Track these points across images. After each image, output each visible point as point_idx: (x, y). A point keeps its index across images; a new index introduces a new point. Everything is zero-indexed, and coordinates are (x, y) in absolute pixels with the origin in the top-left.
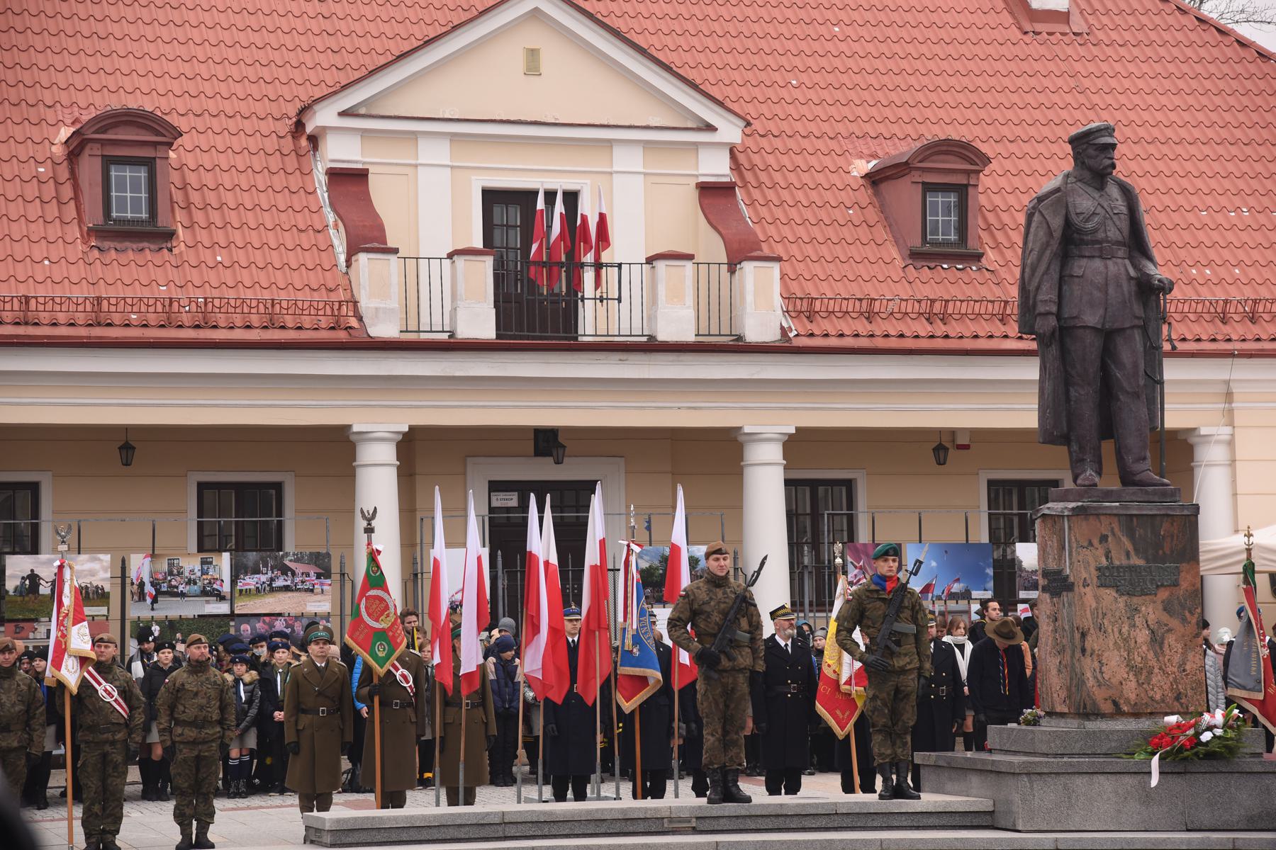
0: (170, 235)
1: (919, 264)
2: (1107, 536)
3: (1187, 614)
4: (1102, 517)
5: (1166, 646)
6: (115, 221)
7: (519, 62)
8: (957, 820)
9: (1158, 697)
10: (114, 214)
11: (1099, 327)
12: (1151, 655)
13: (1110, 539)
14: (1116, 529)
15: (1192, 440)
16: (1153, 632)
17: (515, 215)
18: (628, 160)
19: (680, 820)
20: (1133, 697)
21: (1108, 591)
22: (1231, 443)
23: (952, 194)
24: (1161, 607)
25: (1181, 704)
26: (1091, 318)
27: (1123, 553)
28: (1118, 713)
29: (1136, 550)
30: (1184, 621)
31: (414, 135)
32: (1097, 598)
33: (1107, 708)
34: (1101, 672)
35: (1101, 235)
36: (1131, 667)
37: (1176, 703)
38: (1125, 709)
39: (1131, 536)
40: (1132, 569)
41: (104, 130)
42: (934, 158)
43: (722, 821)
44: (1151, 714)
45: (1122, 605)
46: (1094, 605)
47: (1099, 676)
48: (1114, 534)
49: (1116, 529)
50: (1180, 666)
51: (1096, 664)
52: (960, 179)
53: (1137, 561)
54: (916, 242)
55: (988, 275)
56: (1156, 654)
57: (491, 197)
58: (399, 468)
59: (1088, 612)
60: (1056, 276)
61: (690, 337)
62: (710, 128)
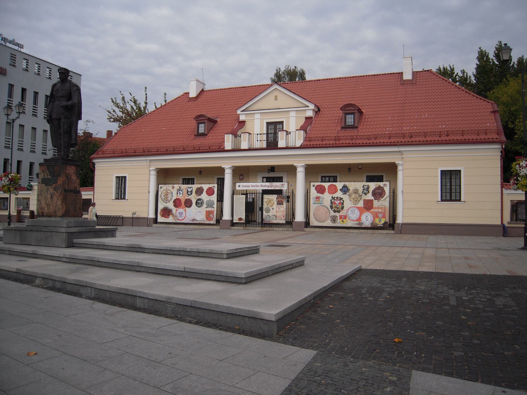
1: (344, 129)
2: (44, 171)
4: (44, 166)
6: (199, 133)
9: (51, 212)
12: (50, 201)
13: (45, 172)
14: (46, 169)
16: (51, 195)
18: (293, 114)
20: (46, 211)
21: (44, 185)
23: (353, 115)
24: (53, 188)
25: (55, 214)
32: (41, 186)
34: (41, 205)
36: (46, 204)
37: (54, 214)
38: (45, 215)
40: (48, 179)
42: (347, 108)
45: (45, 188)
46: (40, 188)
47: (40, 206)
49: (46, 169)
50: (56, 204)
51: (40, 203)
53: (50, 177)
54: (343, 125)
56: (51, 201)
57: (268, 124)
61: (285, 146)
62: (308, 107)
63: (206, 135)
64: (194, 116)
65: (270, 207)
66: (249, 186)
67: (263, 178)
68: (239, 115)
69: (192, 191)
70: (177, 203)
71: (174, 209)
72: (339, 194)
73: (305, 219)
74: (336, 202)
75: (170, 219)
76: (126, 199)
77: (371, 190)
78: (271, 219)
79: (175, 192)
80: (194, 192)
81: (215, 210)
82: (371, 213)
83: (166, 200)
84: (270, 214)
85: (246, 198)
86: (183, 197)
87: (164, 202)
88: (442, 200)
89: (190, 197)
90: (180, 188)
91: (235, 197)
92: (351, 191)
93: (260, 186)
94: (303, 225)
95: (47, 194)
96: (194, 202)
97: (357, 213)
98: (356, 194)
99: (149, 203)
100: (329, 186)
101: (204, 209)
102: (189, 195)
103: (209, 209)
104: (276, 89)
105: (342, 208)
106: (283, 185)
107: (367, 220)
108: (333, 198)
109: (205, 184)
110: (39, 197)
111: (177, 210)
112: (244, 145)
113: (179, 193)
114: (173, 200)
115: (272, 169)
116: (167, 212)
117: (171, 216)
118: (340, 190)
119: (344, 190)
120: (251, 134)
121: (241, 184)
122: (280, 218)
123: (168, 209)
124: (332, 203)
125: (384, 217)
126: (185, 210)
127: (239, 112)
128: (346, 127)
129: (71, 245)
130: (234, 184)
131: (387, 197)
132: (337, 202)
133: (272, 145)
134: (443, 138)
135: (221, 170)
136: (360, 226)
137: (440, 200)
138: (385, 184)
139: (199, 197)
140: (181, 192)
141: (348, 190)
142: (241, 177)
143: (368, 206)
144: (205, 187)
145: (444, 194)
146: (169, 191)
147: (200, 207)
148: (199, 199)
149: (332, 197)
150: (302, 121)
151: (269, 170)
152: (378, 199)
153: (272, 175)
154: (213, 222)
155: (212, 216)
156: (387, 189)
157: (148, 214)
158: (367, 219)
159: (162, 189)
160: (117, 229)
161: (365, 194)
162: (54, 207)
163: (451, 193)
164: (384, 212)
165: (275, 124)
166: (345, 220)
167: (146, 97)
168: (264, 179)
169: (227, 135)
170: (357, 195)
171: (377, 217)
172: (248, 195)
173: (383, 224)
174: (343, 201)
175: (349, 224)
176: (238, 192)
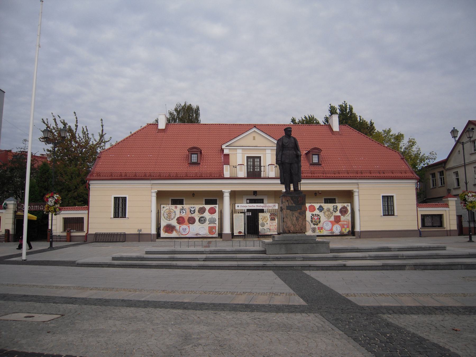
0: (199, 164)
3: (303, 214)
5: (299, 221)
7: (252, 138)
8: (258, 252)
9: (297, 230)
10: (192, 161)
11: (289, 163)
13: (289, 201)
15: (353, 192)
16: (297, 218)
17: (251, 160)
19: (207, 252)
20: (293, 230)
21: (288, 210)
22: (358, 192)
24: (298, 213)
26: (287, 161)
27: (292, 204)
28: (289, 232)
29: (294, 203)
30: (303, 216)
32: (286, 212)
33: (287, 231)
34: (287, 225)
35: (289, 146)
38: (291, 232)
39: (293, 201)
43: (214, 252)
44: (296, 233)
45: (291, 213)
47: (286, 226)
48: (290, 200)
52: (318, 153)
53: (294, 205)
54: (311, 163)
55: (322, 167)
56: (297, 222)
58: (230, 197)
59: (284, 214)
60: (281, 154)
65: (265, 222)
66: (247, 207)
69: (195, 210)
70: (180, 221)
71: (178, 226)
72: (317, 212)
73: (231, 232)
74: (315, 218)
75: (174, 234)
76: (126, 217)
77: (339, 208)
78: (266, 231)
79: (178, 211)
80: (197, 211)
81: (217, 225)
82: (340, 225)
83: (169, 218)
84: (265, 228)
87: (167, 220)
88: (384, 215)
89: (193, 215)
90: (183, 208)
91: (234, 215)
92: (325, 209)
93: (256, 206)
94: (156, 236)
95: (293, 217)
96: (197, 219)
97: (330, 225)
98: (329, 212)
99: (151, 221)
100: (310, 206)
101: (206, 225)
102: (193, 214)
105: (320, 222)
106: (274, 205)
107: (337, 230)
108: (313, 215)
109: (197, 204)
110: (284, 219)
111: (180, 227)
113: (182, 212)
114: (176, 218)
115: (255, 193)
116: (170, 228)
117: (174, 232)
118: (317, 209)
119: (320, 209)
121: (239, 205)
122: (273, 231)
123: (172, 226)
124: (312, 218)
125: (348, 227)
126: (189, 227)
127: (224, 147)
130: (232, 205)
131: (349, 214)
132: (316, 218)
134: (382, 175)
135: (220, 194)
136: (332, 234)
138: (348, 205)
139: (202, 215)
140: (184, 211)
141: (323, 209)
143: (337, 220)
146: (172, 211)
147: (203, 223)
148: (202, 217)
149: (312, 214)
152: (343, 215)
154: (216, 235)
155: (215, 231)
157: (151, 231)
158: (337, 229)
159: (165, 209)
161: (335, 212)
162: (300, 226)
163: (388, 210)
164: (348, 224)
165: (254, 158)
166: (321, 231)
167: (77, 121)
168: (247, 200)
169: (226, 165)
170: (330, 213)
171: (344, 227)
173: (348, 232)
174: (320, 217)
175: (325, 233)
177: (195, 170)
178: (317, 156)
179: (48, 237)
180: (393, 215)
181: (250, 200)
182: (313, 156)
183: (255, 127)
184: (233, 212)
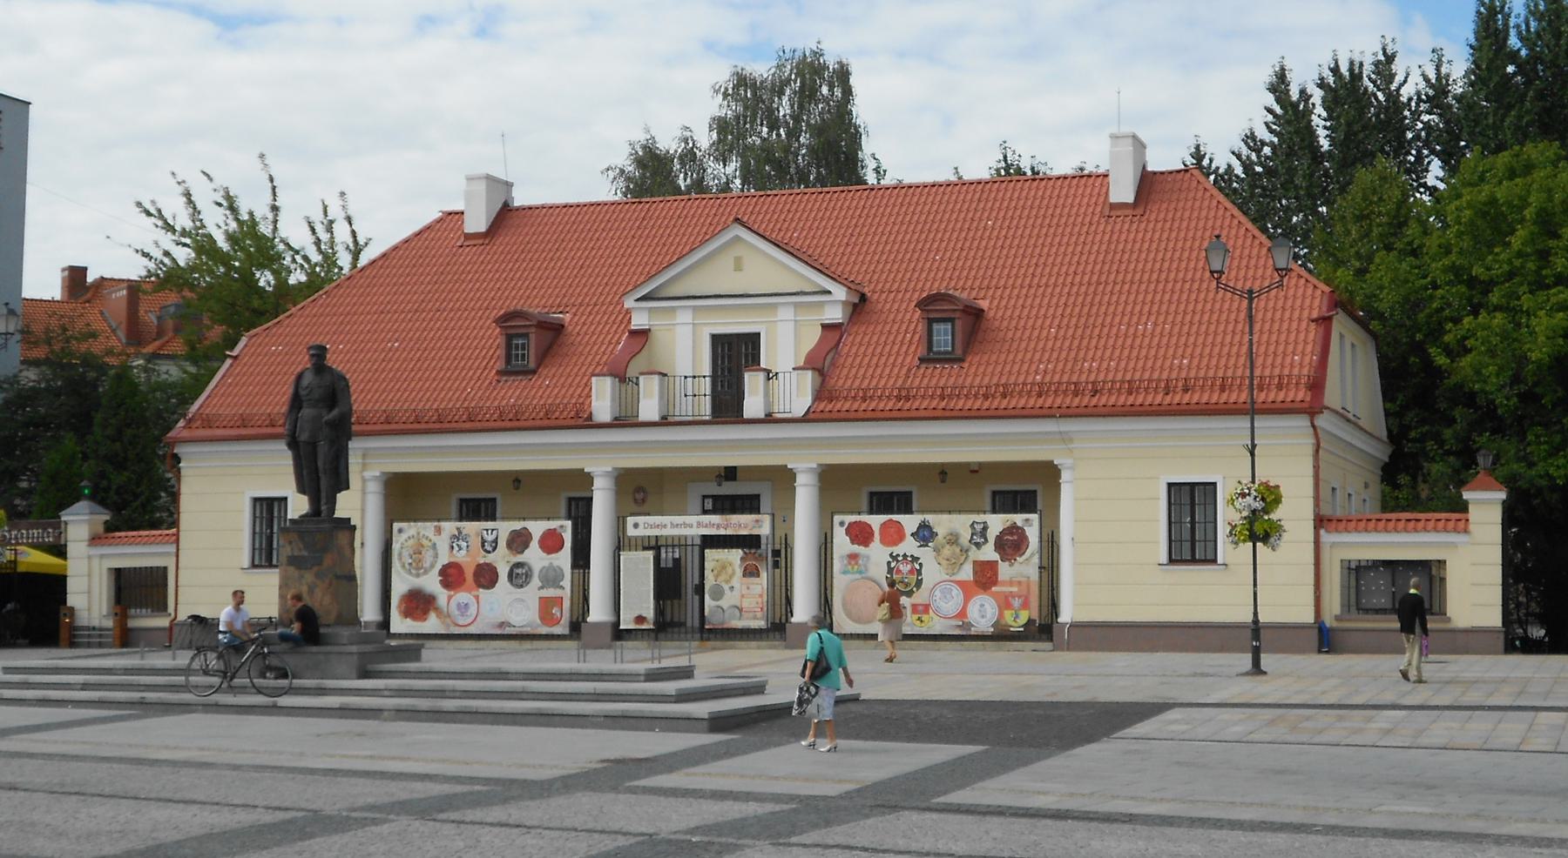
21: (292, 569)
31: (673, 309)
40: (303, 557)
41: (505, 321)
53: (305, 553)
63: (534, 372)
64: (495, 314)
65: (723, 584)
66: (665, 526)
67: (705, 497)
68: (628, 312)
69: (496, 541)
70: (451, 576)
71: (442, 595)
72: (909, 546)
74: (901, 567)
75: (431, 624)
77: (992, 534)
78: (727, 615)
79: (443, 543)
80: (502, 543)
82: (995, 596)
83: (417, 567)
84: (724, 603)
85: (657, 559)
86: (467, 557)
87: (410, 573)
88: (1171, 561)
89: (490, 558)
90: (460, 533)
91: (624, 556)
92: (940, 537)
93: (695, 525)
96: (503, 572)
97: (957, 593)
98: (954, 546)
100: (884, 526)
101: (533, 592)
102: (489, 552)
103: (551, 592)
104: (737, 239)
105: (919, 583)
106: (757, 521)
107: (983, 617)
108: (894, 557)
111: (450, 598)
112: (649, 409)
113: (456, 548)
114: (438, 567)
115: (730, 473)
116: (419, 603)
117: (432, 616)
118: (912, 535)
119: (921, 534)
120: (665, 375)
121: (641, 519)
122: (751, 615)
124: (890, 570)
125: (1025, 605)
126: (477, 598)
127: (629, 303)
128: (930, 358)
129: (365, 674)
131: (1033, 554)
132: (904, 568)
133: (727, 406)
136: (964, 633)
137: (1164, 558)
138: (1027, 520)
139: (520, 558)
140: (464, 544)
141: (933, 535)
142: (640, 496)
143: (985, 577)
144: (537, 528)
145: (1210, 536)
146: (425, 542)
147: (522, 586)
148: (519, 565)
149: (891, 555)
150: (812, 337)
151: (719, 476)
152: (1010, 560)
153: (729, 489)
154: (562, 629)
155: (559, 614)
156: (1033, 534)
158: (983, 613)
159: (404, 536)
160: (422, 646)
161: (978, 545)
164: (1025, 593)
166: (925, 617)
168: (706, 501)
170: (958, 550)
171: (1008, 606)
172: (663, 550)
173: (1025, 626)
174: (921, 565)
175: (935, 625)
176: (633, 543)
177: (513, 393)
178: (949, 326)
179: (64, 634)
180: (1214, 561)
181: (715, 498)
182: (935, 326)
183: (737, 220)
184: (621, 543)
